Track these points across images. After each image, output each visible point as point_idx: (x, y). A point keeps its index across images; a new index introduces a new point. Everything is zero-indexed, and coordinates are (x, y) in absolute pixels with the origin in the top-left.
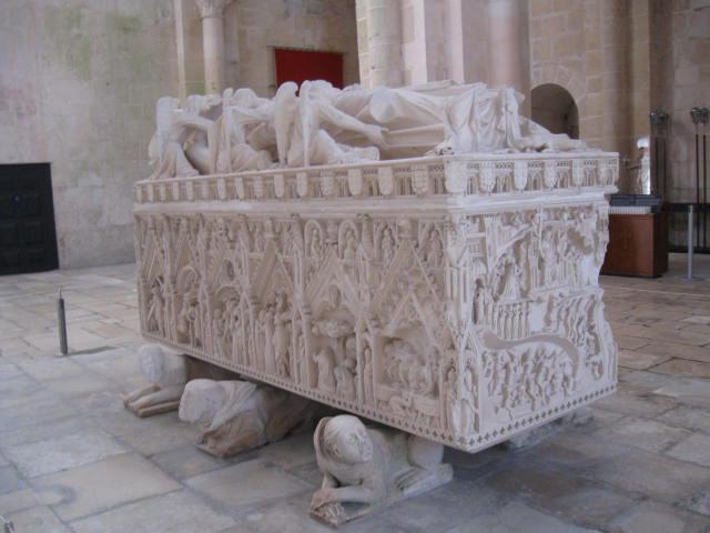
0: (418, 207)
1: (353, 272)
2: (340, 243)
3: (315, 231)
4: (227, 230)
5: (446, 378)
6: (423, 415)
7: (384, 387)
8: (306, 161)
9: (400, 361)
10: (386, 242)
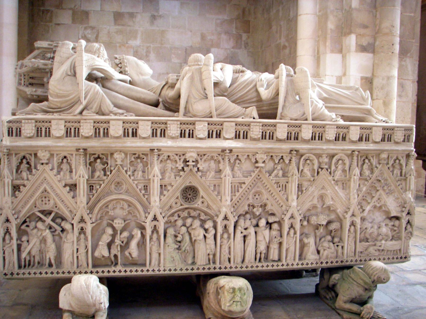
0: (397, 148)
1: (340, 183)
2: (333, 168)
3: (308, 162)
4: (197, 161)
5: (406, 229)
6: (388, 251)
7: (363, 243)
8: (310, 118)
9: (366, 228)
10: (365, 166)
